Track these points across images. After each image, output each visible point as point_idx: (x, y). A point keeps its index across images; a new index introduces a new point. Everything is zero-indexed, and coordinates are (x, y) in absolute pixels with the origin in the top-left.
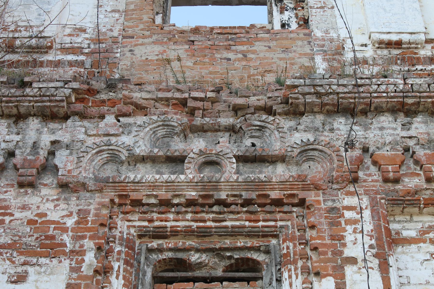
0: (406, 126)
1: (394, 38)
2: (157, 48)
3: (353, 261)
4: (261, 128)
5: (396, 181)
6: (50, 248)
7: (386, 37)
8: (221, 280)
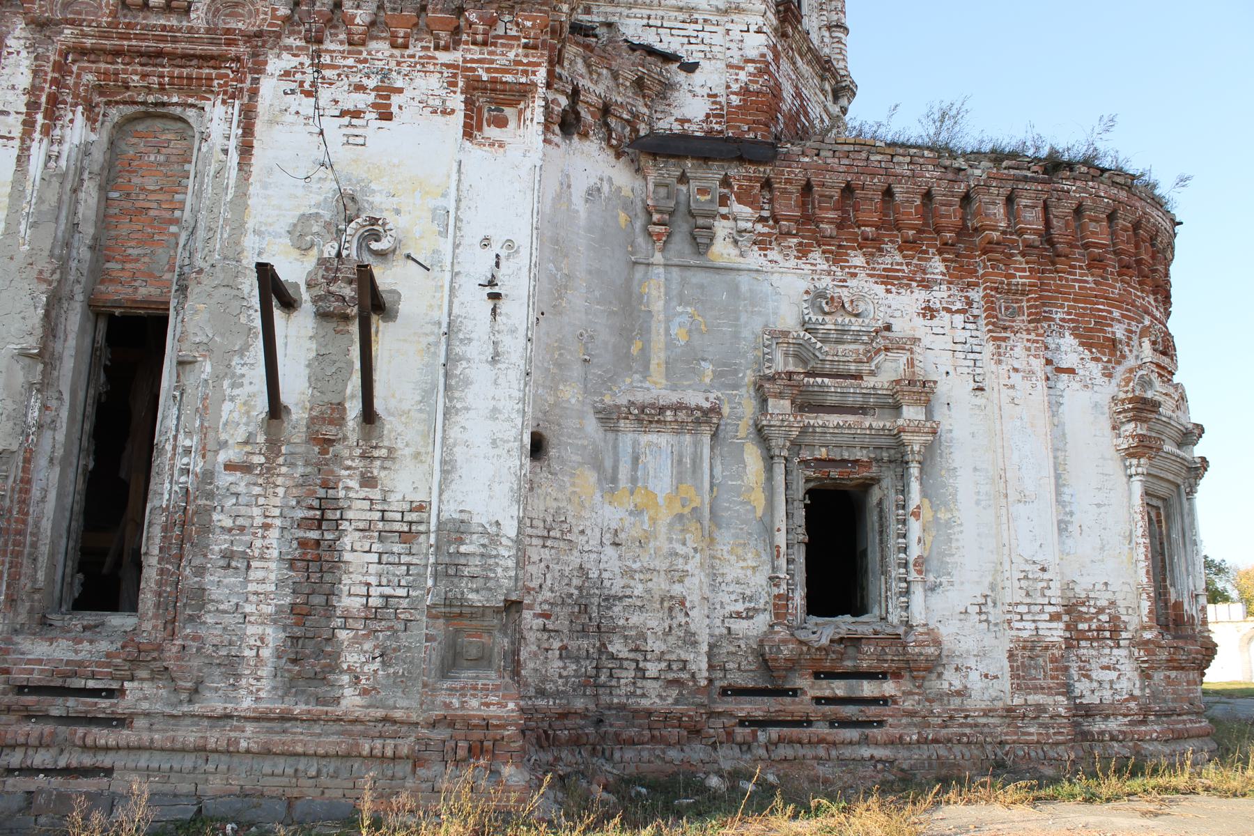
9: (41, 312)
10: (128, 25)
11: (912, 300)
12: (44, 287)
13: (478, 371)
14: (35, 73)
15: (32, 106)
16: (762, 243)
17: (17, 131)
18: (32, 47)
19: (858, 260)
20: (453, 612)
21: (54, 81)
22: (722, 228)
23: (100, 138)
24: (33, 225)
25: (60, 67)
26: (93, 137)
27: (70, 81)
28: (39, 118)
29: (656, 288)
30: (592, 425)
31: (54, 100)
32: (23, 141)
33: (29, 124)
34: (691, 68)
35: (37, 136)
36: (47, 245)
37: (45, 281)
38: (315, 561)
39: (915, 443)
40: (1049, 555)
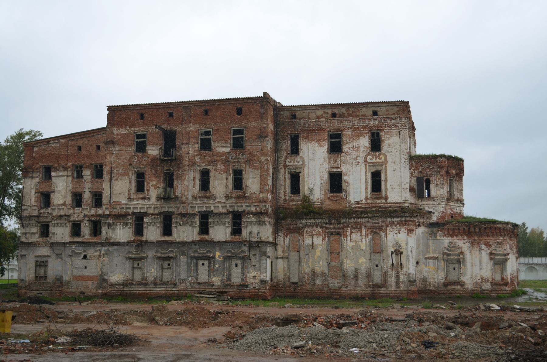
6: (320, 234)
11: (462, 242)
13: (411, 259)
16: (443, 236)
19: (455, 237)
20: (410, 281)
22: (438, 234)
29: (431, 243)
30: (424, 259)
34: (434, 213)
38: (398, 277)
39: (461, 260)
40: (478, 272)
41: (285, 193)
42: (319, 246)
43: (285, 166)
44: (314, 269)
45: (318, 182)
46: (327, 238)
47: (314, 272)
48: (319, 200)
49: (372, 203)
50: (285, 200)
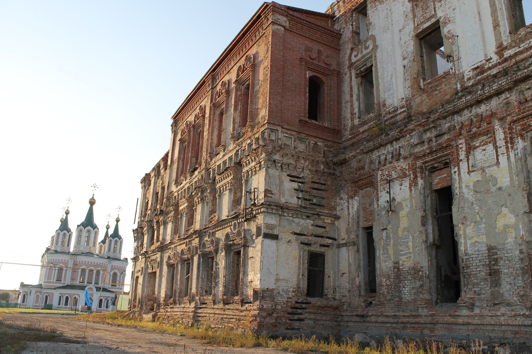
0: (471, 112)
1: (476, 66)
2: (420, 98)
3: (461, 160)
4: (440, 124)
5: (470, 131)
6: (405, 176)
7: (473, 67)
8: (443, 168)
9: (526, 199)
10: (524, 109)
12: (525, 192)
14: (504, 133)
15: (506, 142)
17: (505, 152)
18: (501, 126)
21: (510, 133)
23: (527, 143)
24: (517, 175)
25: (510, 129)
26: (526, 144)
27: (514, 131)
28: (509, 145)
31: (511, 138)
32: (507, 153)
33: (507, 148)
35: (510, 150)
36: (522, 180)
37: (525, 190)
41: (352, 114)
42: (404, 204)
43: (351, 65)
44: (397, 263)
45: (400, 63)
46: (420, 182)
47: (398, 269)
48: (404, 102)
49: (516, 54)
50: (353, 127)
